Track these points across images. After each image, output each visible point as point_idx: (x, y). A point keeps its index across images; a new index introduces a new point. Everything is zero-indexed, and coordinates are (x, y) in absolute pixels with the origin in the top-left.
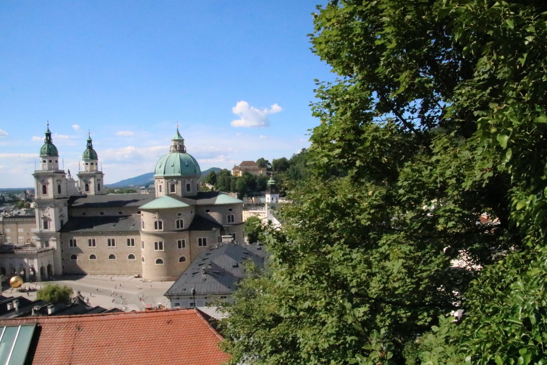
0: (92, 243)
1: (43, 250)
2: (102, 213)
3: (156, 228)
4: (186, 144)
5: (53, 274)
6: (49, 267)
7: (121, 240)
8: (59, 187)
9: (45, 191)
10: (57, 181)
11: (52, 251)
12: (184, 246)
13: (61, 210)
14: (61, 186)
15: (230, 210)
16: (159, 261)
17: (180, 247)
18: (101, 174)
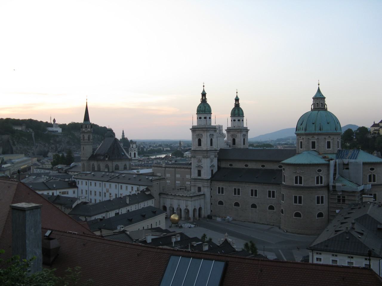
0: (237, 192)
1: (195, 195)
2: (246, 166)
3: (296, 183)
4: (327, 101)
5: (203, 216)
6: (200, 209)
7: (263, 190)
8: (211, 140)
9: (200, 144)
10: (210, 135)
11: (202, 197)
12: (322, 202)
13: (212, 161)
14: (213, 139)
15: (372, 169)
16: (298, 215)
17: (318, 203)
18: (247, 130)
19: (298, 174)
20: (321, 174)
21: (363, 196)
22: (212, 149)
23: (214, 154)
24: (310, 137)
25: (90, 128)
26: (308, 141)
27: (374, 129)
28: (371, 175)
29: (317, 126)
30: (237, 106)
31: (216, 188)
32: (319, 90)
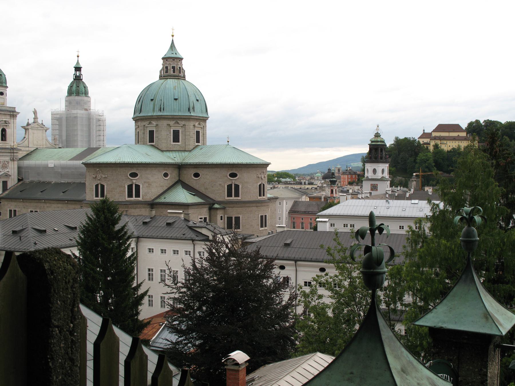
4: (185, 65)
15: (233, 175)
19: (99, 180)
20: (135, 181)
21: (168, 211)
22: (4, 147)
23: (9, 154)
24: (146, 123)
26: (144, 130)
27: (423, 141)
28: (231, 185)
29: (156, 104)
30: (78, 79)
31: (7, 211)
32: (173, 46)
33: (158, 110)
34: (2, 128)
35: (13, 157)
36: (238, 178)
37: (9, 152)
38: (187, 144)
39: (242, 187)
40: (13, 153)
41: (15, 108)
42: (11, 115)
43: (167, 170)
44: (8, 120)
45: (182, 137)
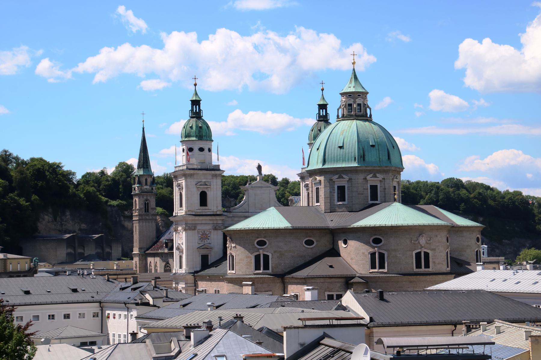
10: (196, 184)
13: (204, 236)
23: (211, 222)
25: (149, 183)
33: (320, 162)
34: (201, 191)
35: (216, 225)
36: (383, 245)
37: (210, 220)
38: (354, 202)
39: (388, 256)
40: (217, 220)
41: (219, 166)
42: (213, 174)
43: (310, 237)
44: (209, 180)
45: (348, 194)
